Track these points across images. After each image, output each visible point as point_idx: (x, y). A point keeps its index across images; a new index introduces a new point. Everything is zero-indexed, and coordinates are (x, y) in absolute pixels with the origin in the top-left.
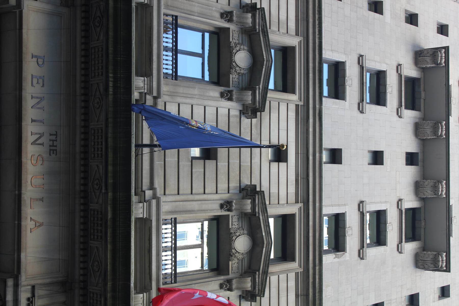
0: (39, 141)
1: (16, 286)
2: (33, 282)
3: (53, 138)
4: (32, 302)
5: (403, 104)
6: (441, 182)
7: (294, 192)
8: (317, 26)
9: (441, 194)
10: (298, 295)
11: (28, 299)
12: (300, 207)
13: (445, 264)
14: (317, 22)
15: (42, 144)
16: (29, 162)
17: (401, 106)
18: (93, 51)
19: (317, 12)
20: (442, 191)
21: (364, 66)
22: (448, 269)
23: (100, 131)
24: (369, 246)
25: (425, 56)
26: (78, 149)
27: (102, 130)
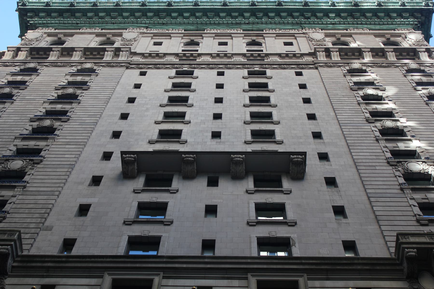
5: (167, 188)
6: (233, 158)
7: (238, 281)
8: (96, 260)
9: (242, 158)
10: (327, 278)
12: (251, 275)
13: (299, 156)
14: (93, 260)
17: (168, 190)
19: (84, 260)
20: (239, 158)
21: (132, 220)
22: (304, 154)
24: (285, 217)
25: (128, 171)
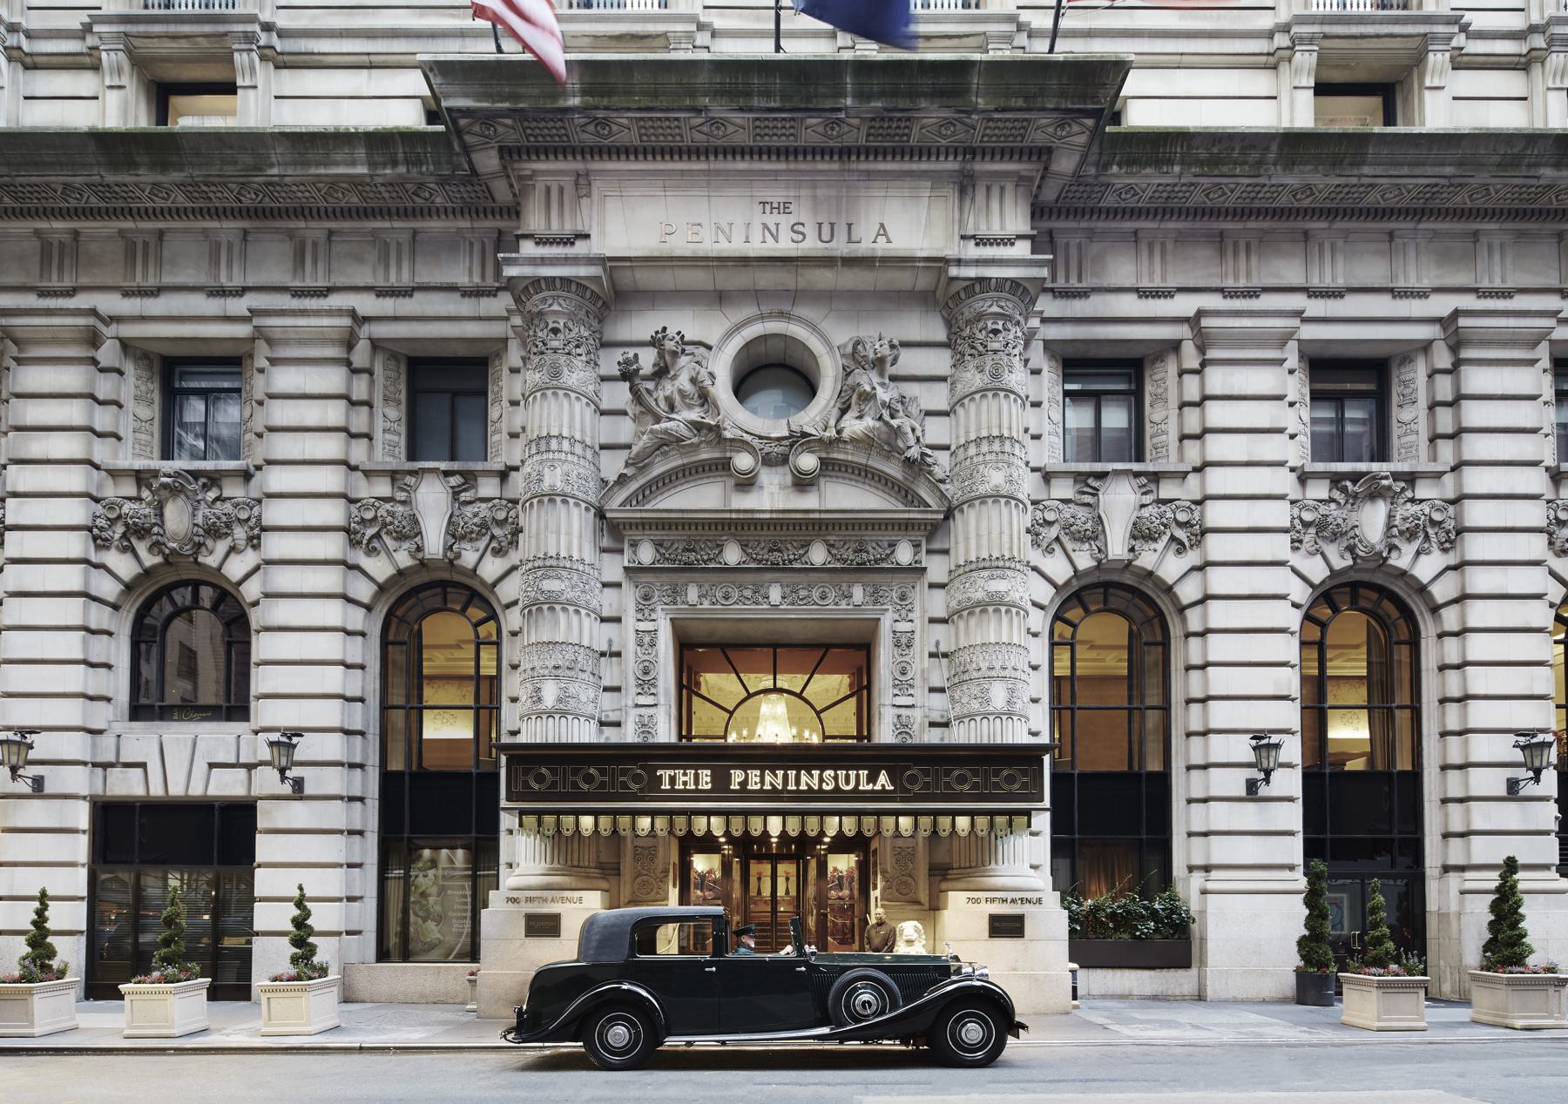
0: (773, 230)
1: (959, 262)
2: (957, 237)
3: (768, 207)
4: (981, 239)
11: (977, 244)
15: (777, 225)
16: (801, 245)
18: (645, 138)
23: (758, 123)
26: (782, 166)
27: (758, 119)
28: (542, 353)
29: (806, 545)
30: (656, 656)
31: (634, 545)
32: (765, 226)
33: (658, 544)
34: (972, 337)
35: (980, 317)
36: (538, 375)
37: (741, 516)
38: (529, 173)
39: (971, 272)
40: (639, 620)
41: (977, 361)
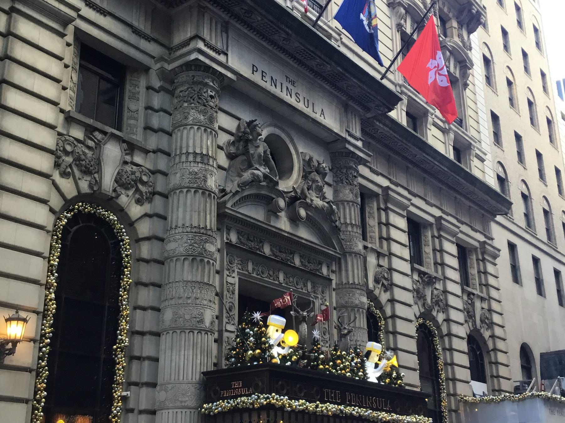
28: (205, 106)
29: (292, 253)
30: (235, 300)
31: (229, 230)
32: (287, 88)
33: (239, 233)
34: (347, 174)
35: (351, 168)
36: (202, 118)
37: (277, 231)
38: (204, 6)
39: (352, 149)
40: (228, 275)
41: (350, 187)
